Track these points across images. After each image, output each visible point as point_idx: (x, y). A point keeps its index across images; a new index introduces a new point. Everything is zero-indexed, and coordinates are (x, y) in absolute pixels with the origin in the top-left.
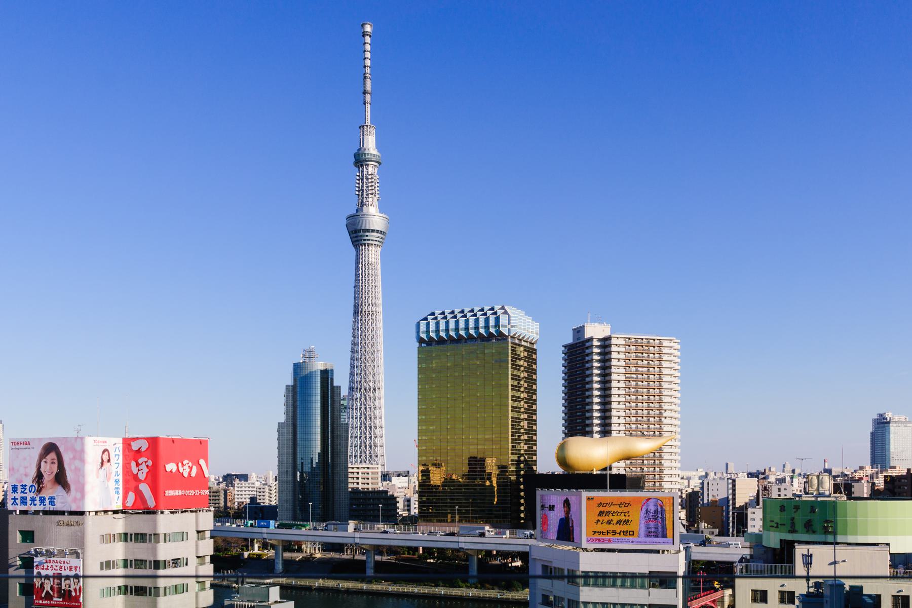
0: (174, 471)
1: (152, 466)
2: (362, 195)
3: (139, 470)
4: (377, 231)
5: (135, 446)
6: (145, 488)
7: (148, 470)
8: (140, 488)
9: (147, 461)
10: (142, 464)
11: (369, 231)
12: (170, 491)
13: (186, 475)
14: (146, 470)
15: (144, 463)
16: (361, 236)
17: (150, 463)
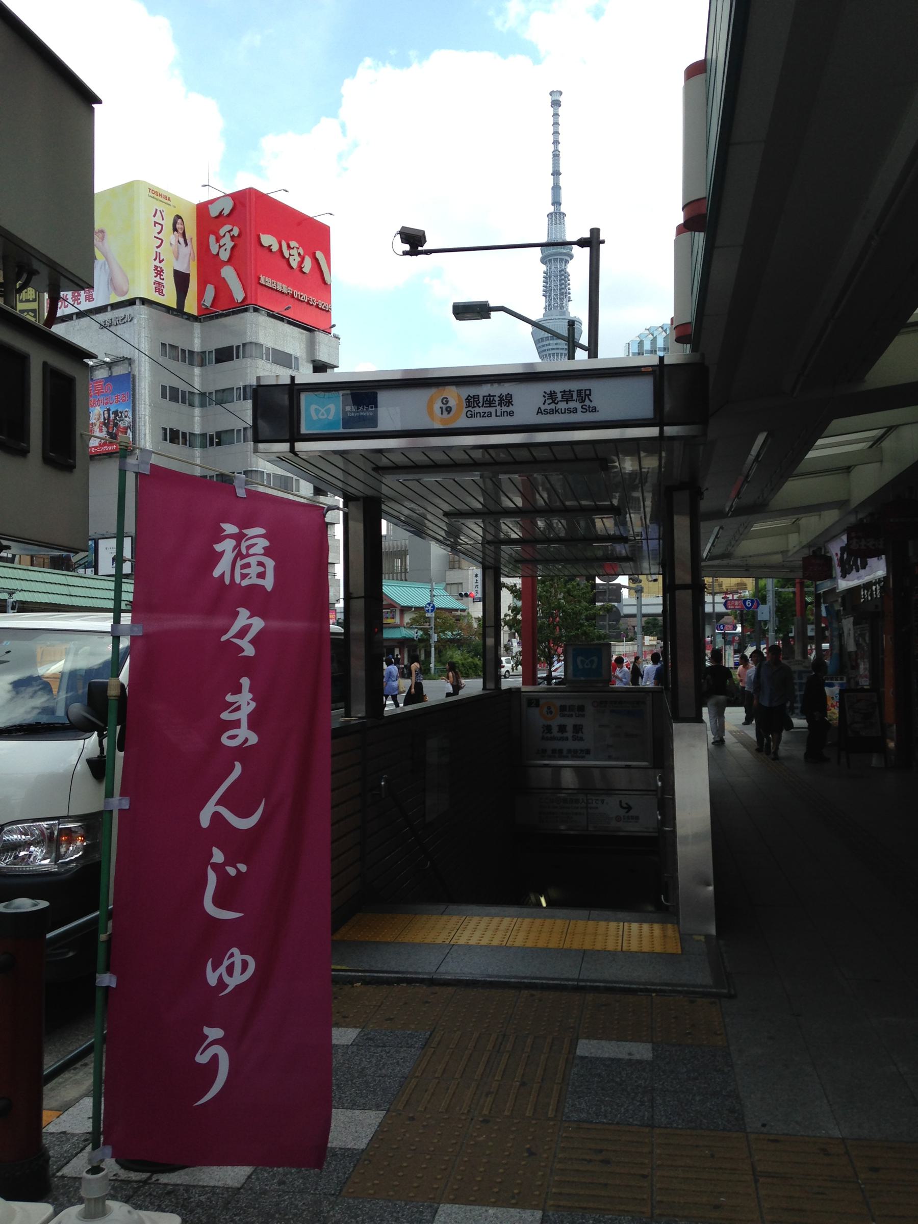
0: (275, 248)
1: (239, 235)
2: (550, 296)
3: (220, 247)
5: (214, 211)
6: (229, 274)
7: (233, 244)
8: (223, 275)
9: (232, 230)
10: (224, 236)
12: (269, 280)
13: (294, 264)
14: (230, 244)
15: (228, 234)
16: (549, 345)
17: (236, 232)
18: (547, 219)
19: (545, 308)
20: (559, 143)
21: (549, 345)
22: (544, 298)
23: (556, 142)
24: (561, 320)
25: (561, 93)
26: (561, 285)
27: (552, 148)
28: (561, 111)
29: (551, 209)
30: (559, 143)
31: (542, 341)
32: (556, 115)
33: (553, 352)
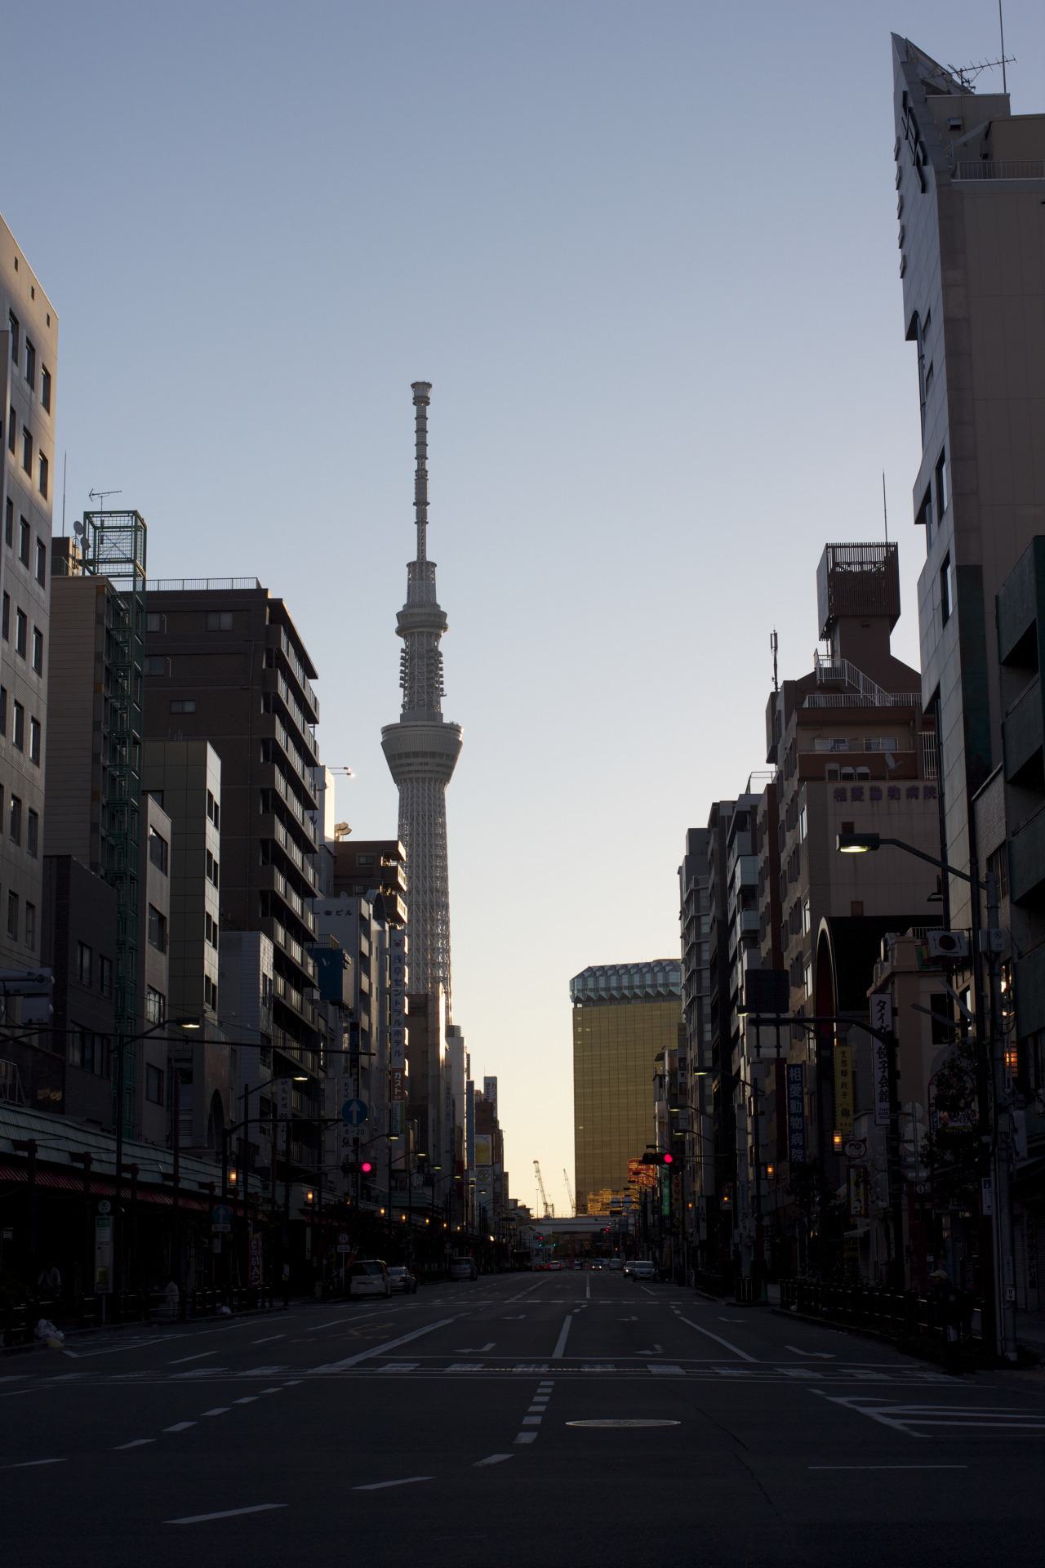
4: (441, 755)
11: (425, 754)
16: (410, 764)
18: (407, 569)
19: (403, 706)
20: (427, 458)
21: (410, 764)
22: (402, 689)
23: (421, 457)
24: (432, 729)
25: (429, 385)
26: (430, 672)
27: (414, 465)
28: (430, 411)
29: (414, 558)
30: (427, 458)
31: (400, 758)
32: (421, 418)
33: (419, 775)
